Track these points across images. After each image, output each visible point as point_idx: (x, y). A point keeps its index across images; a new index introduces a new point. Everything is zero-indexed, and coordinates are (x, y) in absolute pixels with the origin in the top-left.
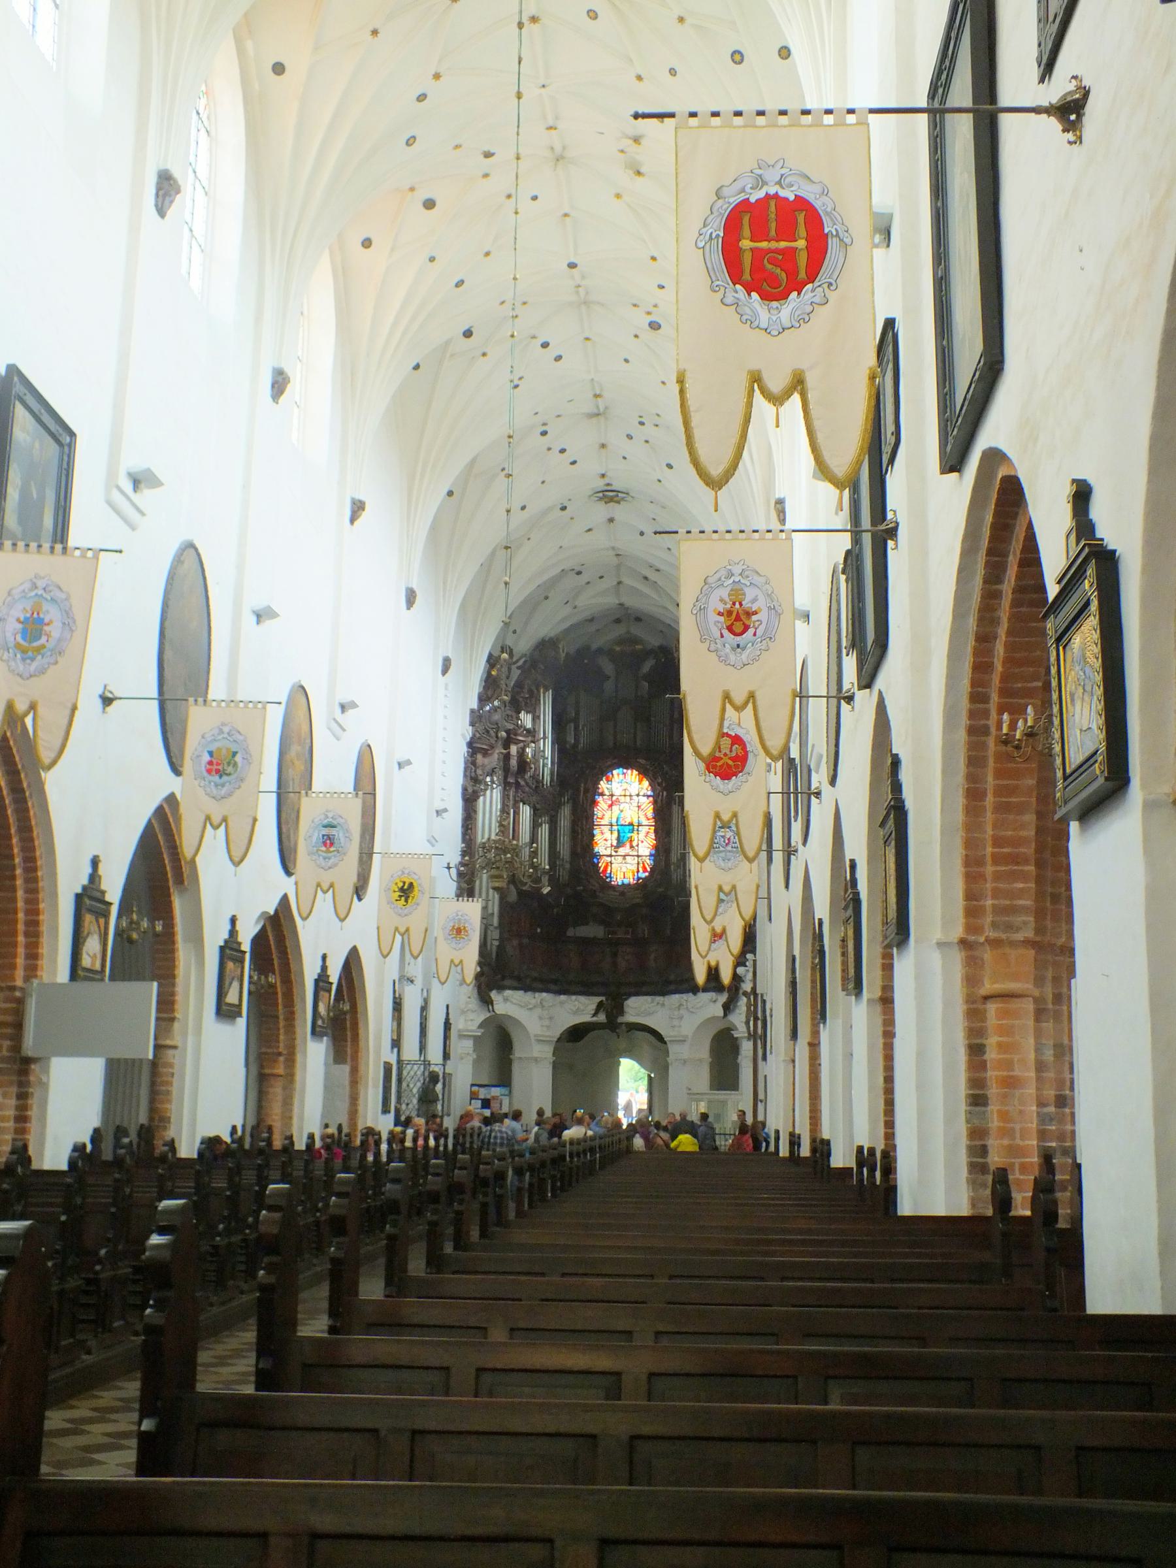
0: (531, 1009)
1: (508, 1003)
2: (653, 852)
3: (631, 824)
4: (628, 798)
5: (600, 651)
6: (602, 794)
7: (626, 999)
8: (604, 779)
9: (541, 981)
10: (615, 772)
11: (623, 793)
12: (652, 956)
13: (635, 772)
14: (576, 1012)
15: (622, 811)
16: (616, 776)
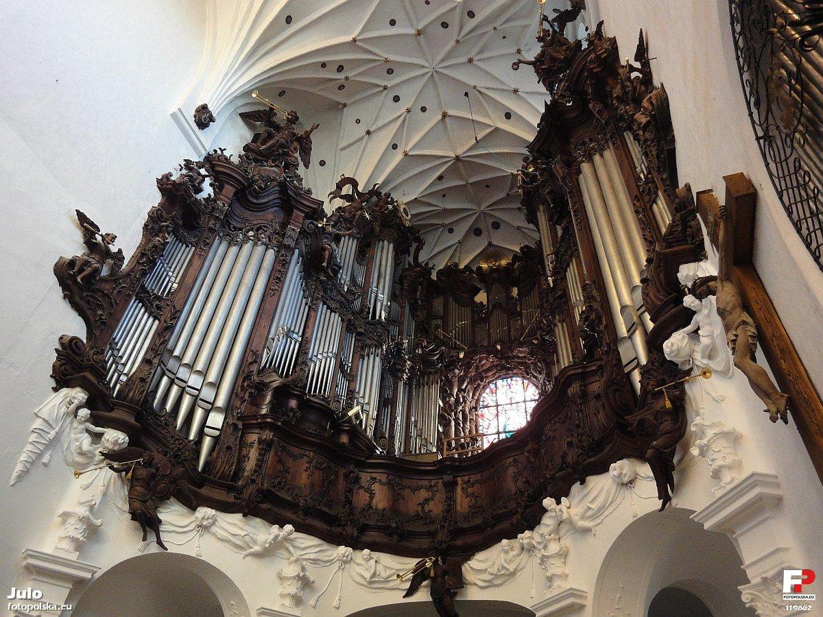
0: (257, 555)
1: (207, 536)
6: (487, 406)
7: (468, 558)
8: (488, 390)
9: (293, 506)
10: (499, 382)
12: (511, 471)
14: (373, 582)
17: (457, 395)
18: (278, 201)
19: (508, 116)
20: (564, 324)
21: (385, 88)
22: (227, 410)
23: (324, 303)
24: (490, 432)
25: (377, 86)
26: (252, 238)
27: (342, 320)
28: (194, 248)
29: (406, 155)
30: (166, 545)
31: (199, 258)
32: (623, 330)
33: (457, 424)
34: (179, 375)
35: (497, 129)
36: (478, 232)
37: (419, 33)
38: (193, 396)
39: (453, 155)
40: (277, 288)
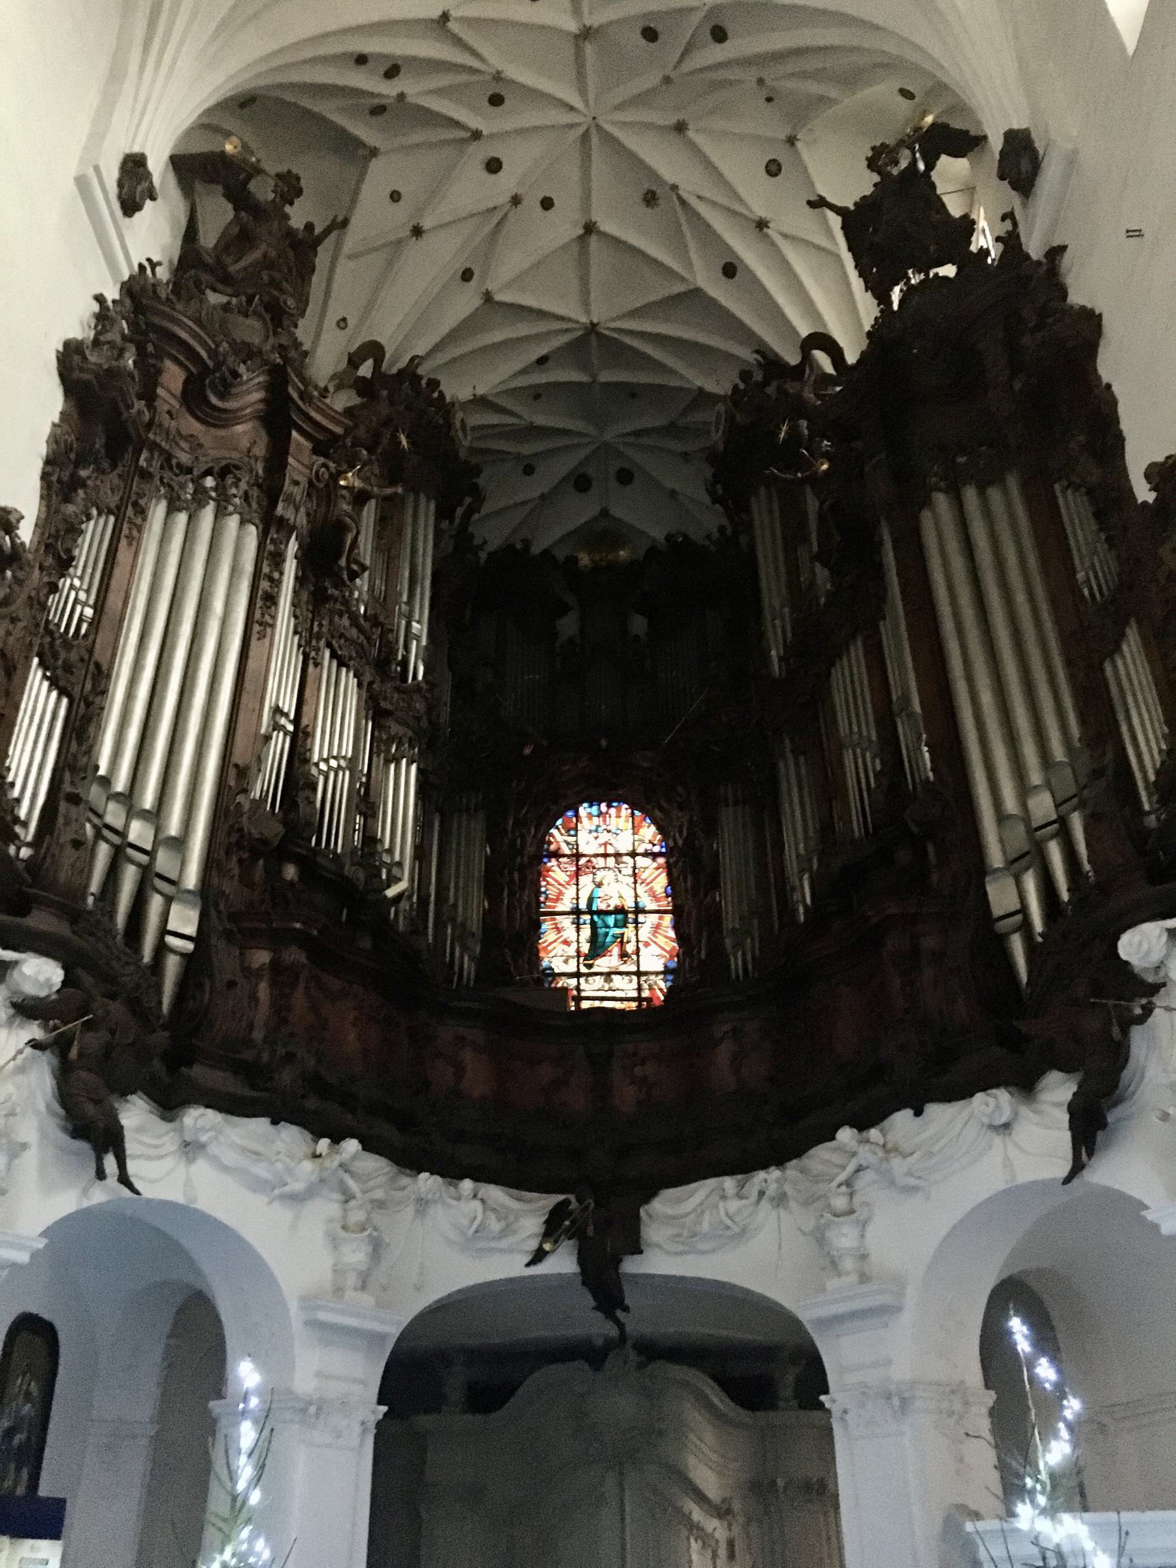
2: (673, 964)
3: (620, 910)
4: (611, 861)
5: (546, 553)
6: (557, 855)
8: (559, 822)
10: (584, 810)
11: (601, 851)
12: (724, 1053)
13: (625, 809)
15: (599, 885)
16: (585, 820)
17: (513, 831)
18: (261, 406)
19: (730, 270)
20: (802, 759)
21: (476, 135)
22: (207, 895)
23: (329, 645)
24: (560, 907)
25: (457, 124)
26: (213, 494)
27: (359, 685)
28: (112, 519)
29: (488, 297)
30: (133, 1180)
31: (130, 544)
32: (996, 857)
33: (512, 894)
34: (109, 819)
35: (697, 292)
36: (582, 483)
37: (586, 34)
38: (139, 865)
39: (584, 319)
40: (267, 618)
